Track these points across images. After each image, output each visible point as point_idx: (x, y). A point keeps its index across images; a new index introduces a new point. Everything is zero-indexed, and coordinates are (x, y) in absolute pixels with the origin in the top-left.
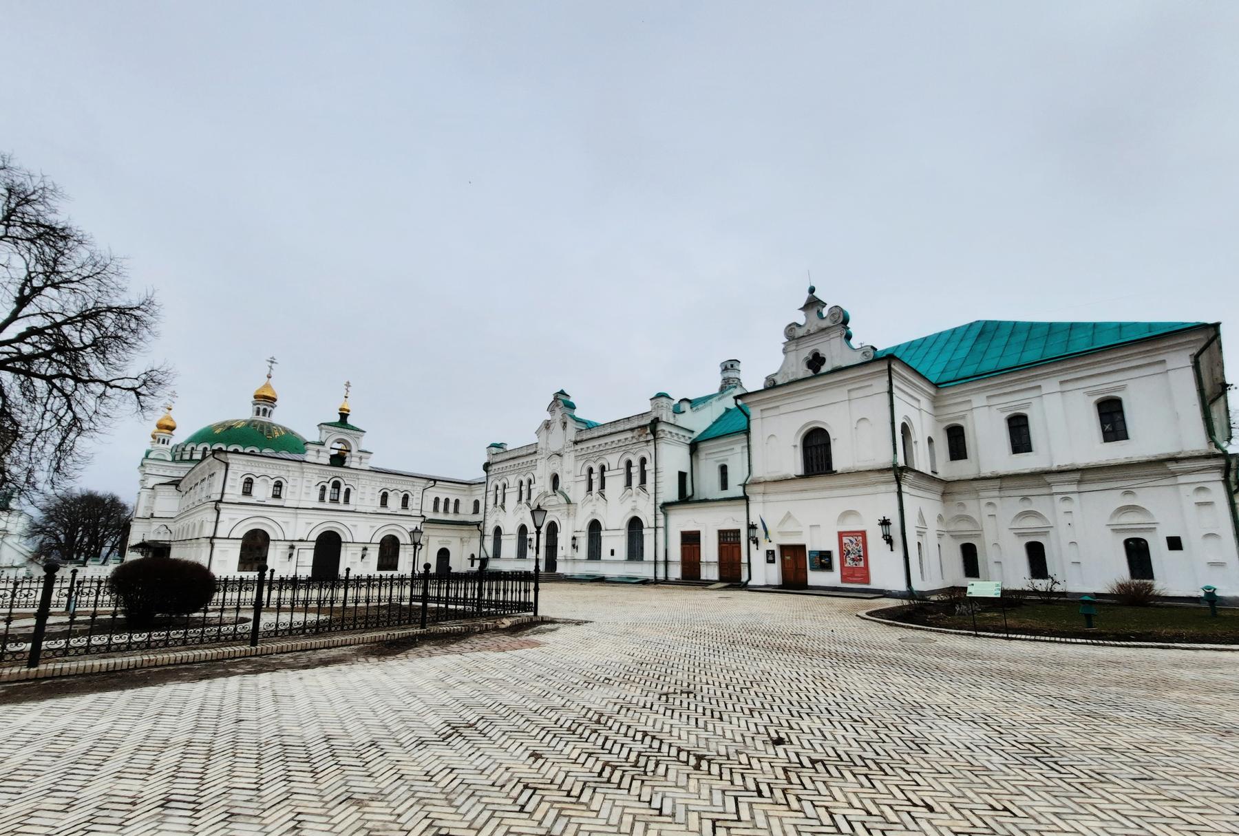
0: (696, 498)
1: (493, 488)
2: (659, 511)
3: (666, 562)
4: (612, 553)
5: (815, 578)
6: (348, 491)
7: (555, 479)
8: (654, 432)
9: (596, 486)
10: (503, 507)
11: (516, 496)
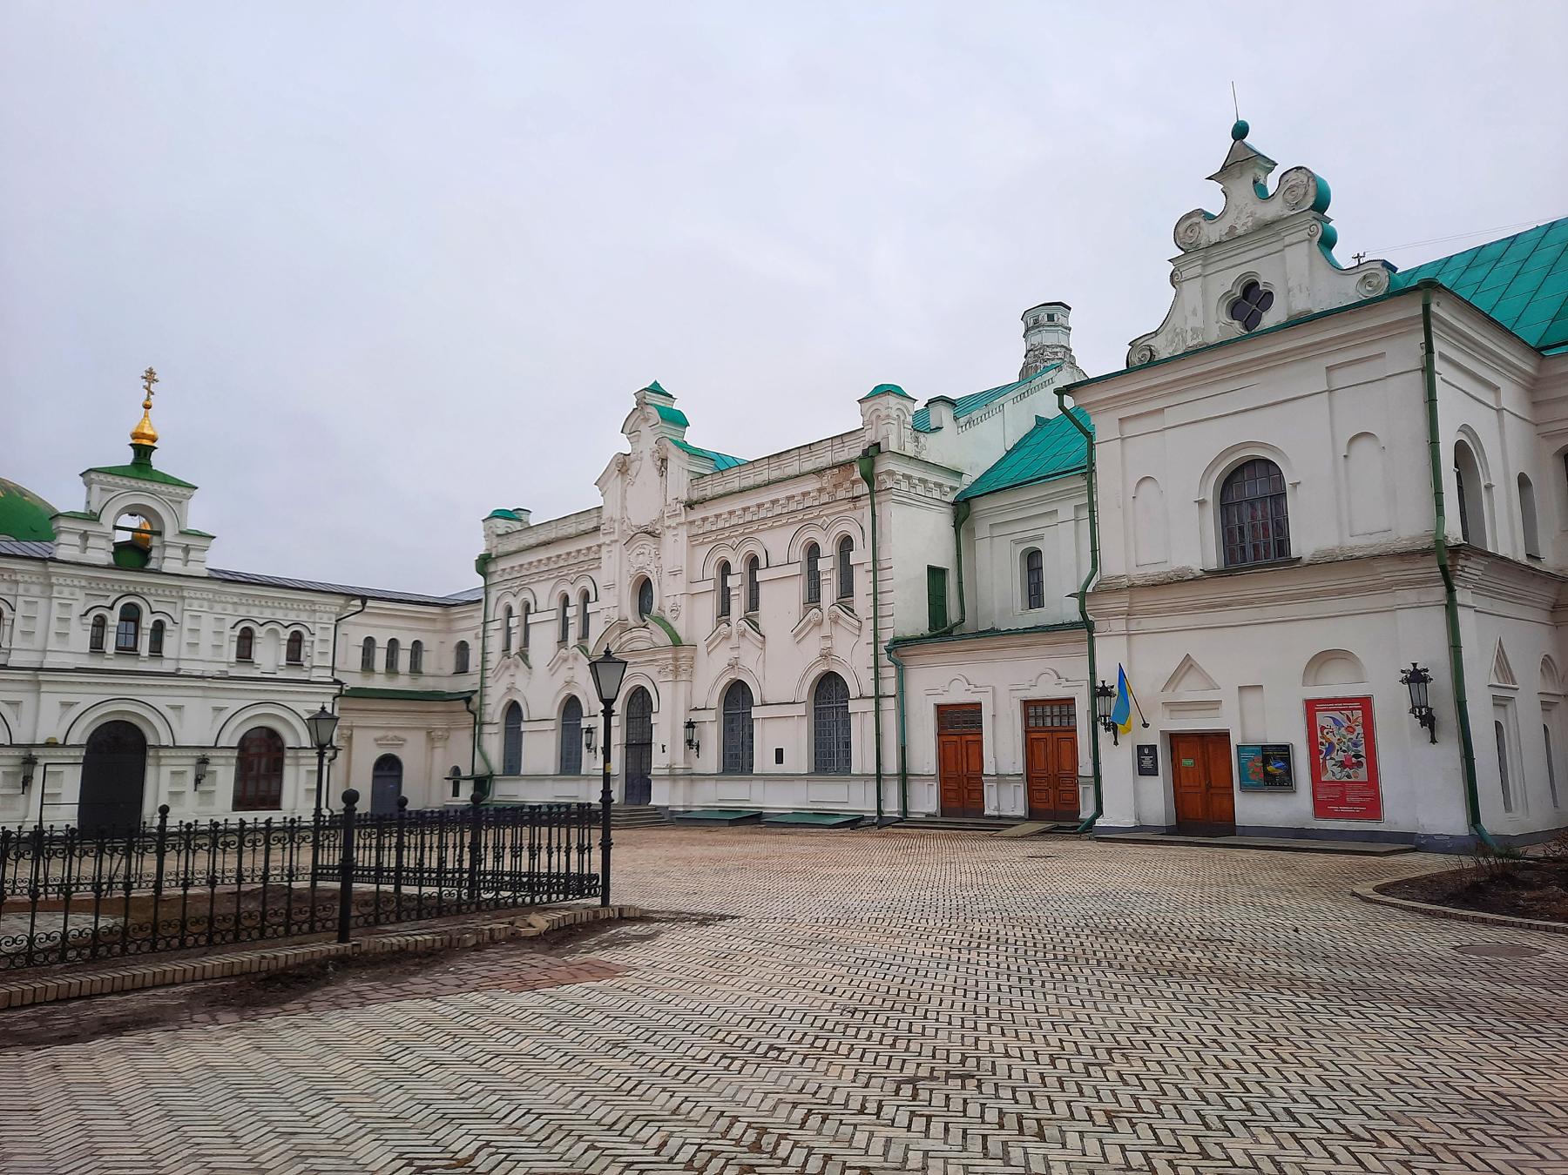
0: (968, 625)
1: (501, 614)
2: (884, 660)
3: (904, 776)
5: (1252, 808)
6: (159, 628)
8: (869, 478)
9: (738, 606)
10: (524, 655)
11: (553, 631)
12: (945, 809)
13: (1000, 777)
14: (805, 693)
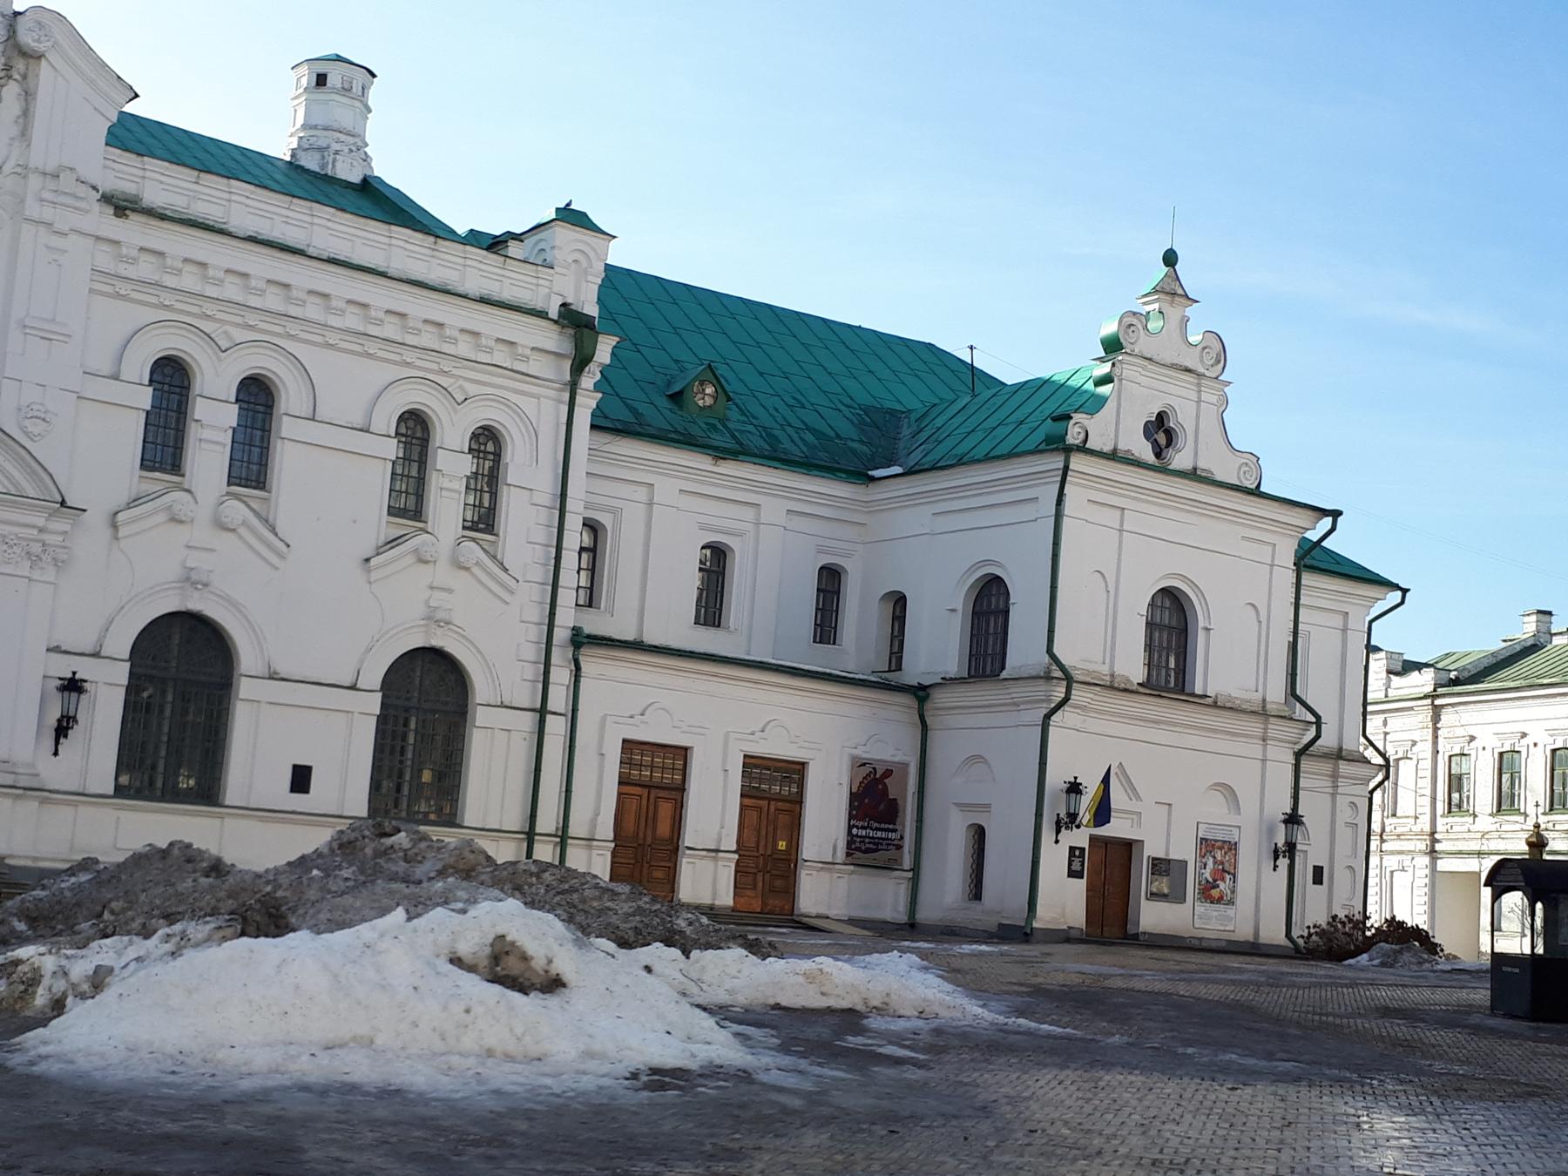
2: (561, 657)
4: (301, 779)
14: (374, 676)
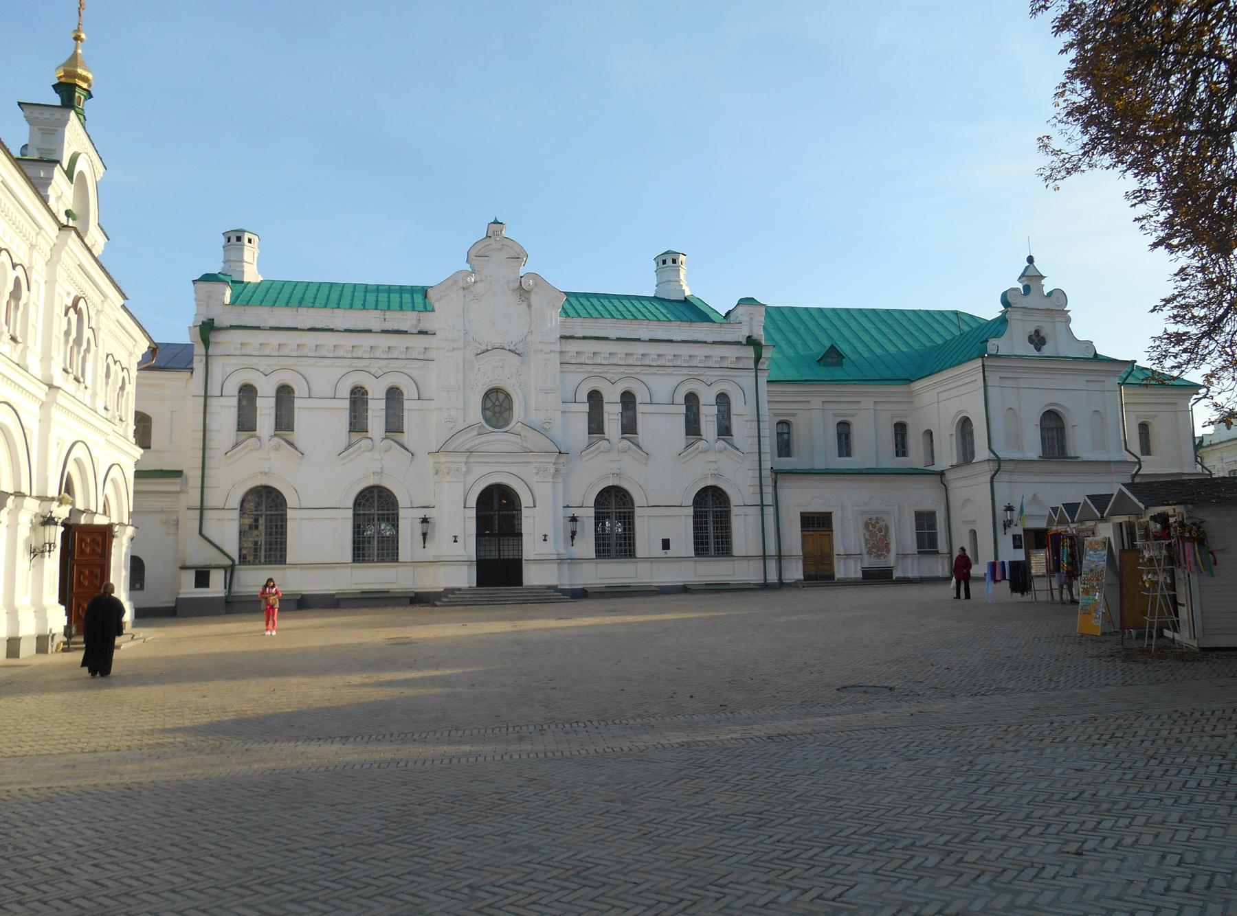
1: (232, 388)
2: (768, 481)
3: (780, 557)
4: (666, 544)
7: (497, 405)
12: (808, 577)
13: (848, 556)
